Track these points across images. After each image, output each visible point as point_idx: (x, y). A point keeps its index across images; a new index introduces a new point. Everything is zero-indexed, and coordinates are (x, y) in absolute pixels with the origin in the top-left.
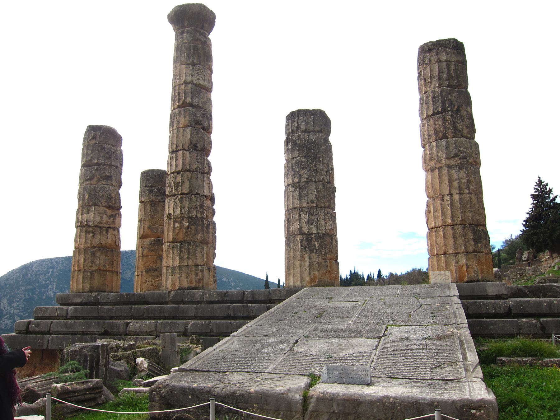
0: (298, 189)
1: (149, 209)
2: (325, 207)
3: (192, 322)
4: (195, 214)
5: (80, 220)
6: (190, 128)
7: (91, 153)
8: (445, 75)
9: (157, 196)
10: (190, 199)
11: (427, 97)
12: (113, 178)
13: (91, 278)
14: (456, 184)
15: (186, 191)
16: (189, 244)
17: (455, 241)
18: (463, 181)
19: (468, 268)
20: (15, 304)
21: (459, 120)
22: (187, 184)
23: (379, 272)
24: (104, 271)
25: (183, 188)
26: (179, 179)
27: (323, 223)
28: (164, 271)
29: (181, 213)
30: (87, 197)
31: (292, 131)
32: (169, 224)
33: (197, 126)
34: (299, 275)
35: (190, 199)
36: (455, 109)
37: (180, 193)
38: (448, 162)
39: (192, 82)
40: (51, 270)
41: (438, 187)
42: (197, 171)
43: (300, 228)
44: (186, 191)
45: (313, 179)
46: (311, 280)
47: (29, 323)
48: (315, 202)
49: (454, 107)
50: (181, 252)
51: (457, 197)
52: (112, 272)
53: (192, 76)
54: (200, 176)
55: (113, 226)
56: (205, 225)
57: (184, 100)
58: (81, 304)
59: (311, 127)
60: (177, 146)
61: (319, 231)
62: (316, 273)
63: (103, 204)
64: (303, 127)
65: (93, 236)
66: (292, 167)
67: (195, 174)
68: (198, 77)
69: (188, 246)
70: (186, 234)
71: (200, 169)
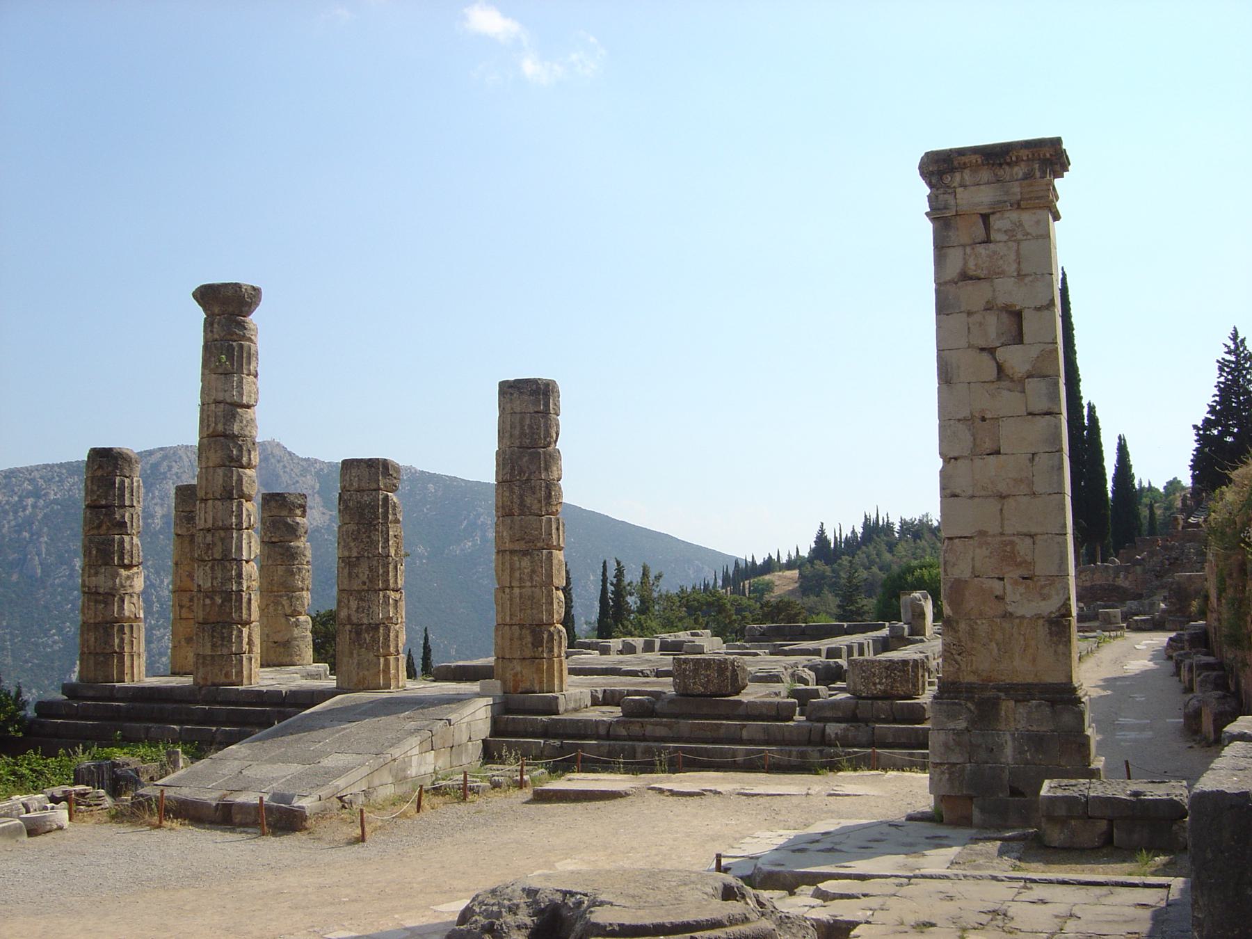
8: (517, 432)
40: (30, 501)
43: (349, 616)
44: (218, 556)
50: (213, 637)
51: (517, 591)
59: (364, 485)
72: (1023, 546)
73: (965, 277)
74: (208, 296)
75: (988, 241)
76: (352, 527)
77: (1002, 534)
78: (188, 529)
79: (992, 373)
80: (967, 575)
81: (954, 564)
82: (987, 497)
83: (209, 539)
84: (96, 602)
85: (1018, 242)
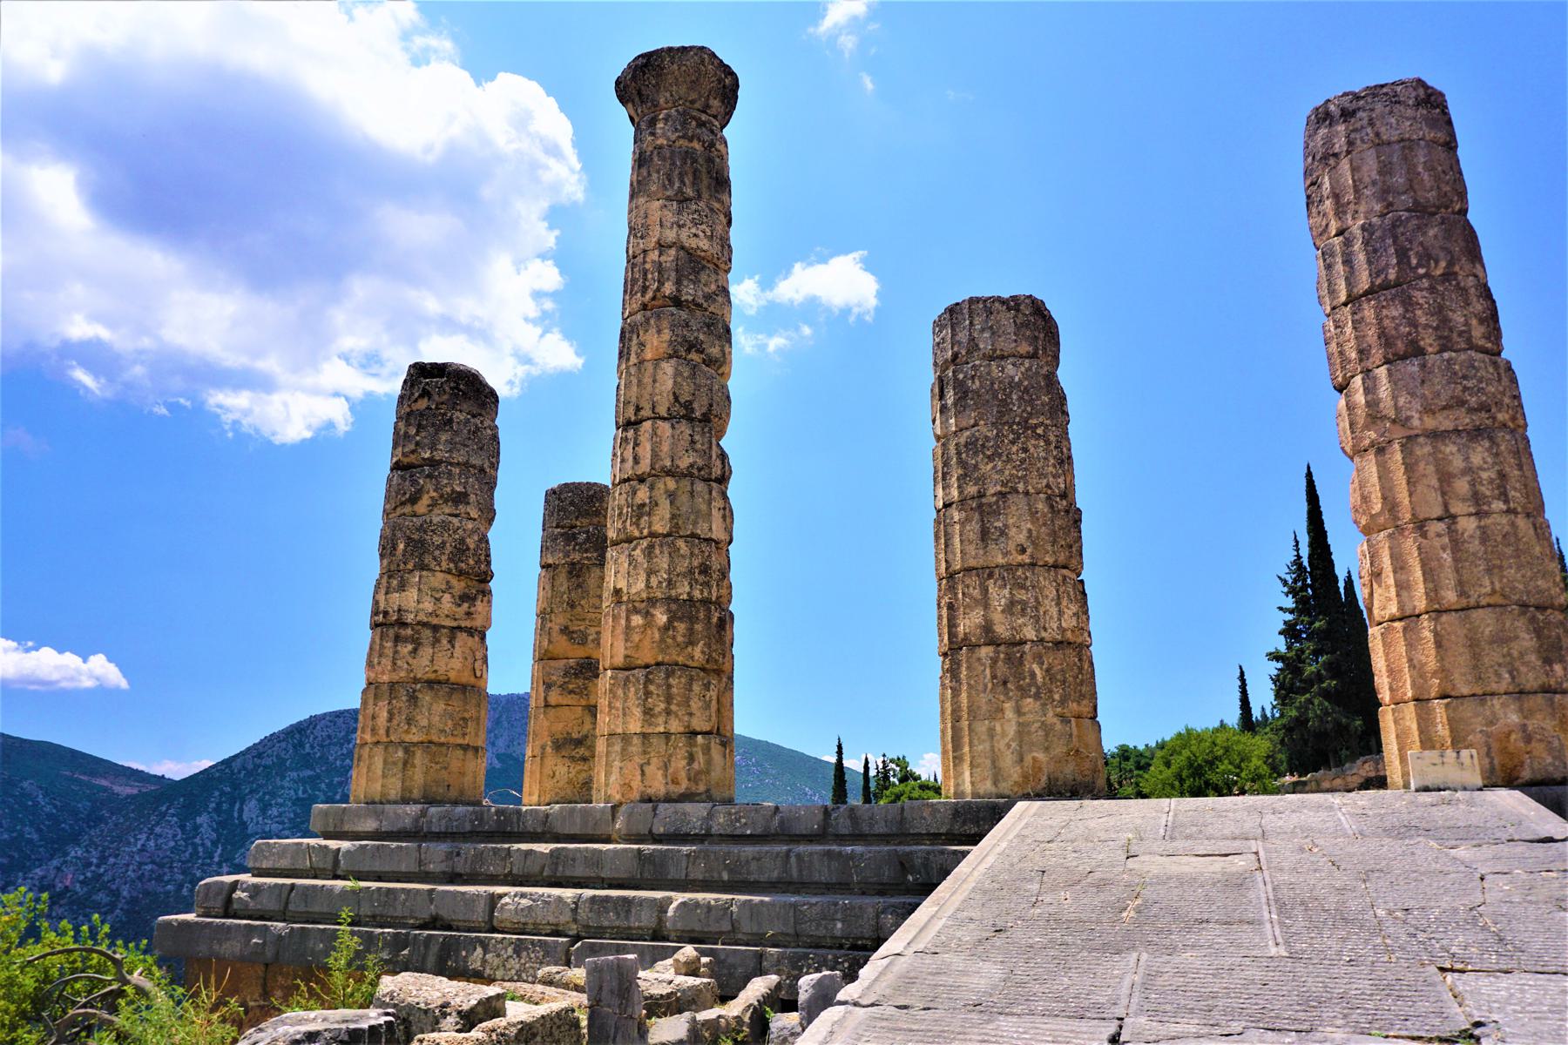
0: (977, 516)
1: (563, 583)
2: (1055, 566)
3: (680, 898)
4: (687, 589)
5: (382, 606)
6: (674, 361)
7: (417, 433)
8: (1399, 180)
9: (586, 551)
10: (673, 552)
11: (1348, 243)
12: (472, 498)
13: (405, 763)
14: (1462, 486)
16: (669, 675)
17: (1476, 657)
18: (1485, 475)
19: (1528, 739)
20: (274, 811)
21: (1452, 301)
22: (664, 510)
24: (442, 744)
25: (655, 519)
27: (1054, 611)
28: (601, 746)
29: (648, 586)
30: (401, 546)
31: (955, 356)
32: (615, 618)
33: (694, 356)
34: (988, 762)
36: (1439, 272)
37: (645, 532)
38: (1430, 423)
41: (1403, 496)
42: (691, 475)
43: (987, 628)
44: (660, 527)
45: (1021, 487)
46: (1025, 777)
48: (1029, 551)
49: (1437, 263)
50: (648, 694)
51: (1468, 525)
52: (465, 748)
53: (680, 227)
54: (700, 487)
55: (468, 624)
56: (715, 620)
57: (658, 289)
58: (376, 835)
60: (638, 409)
61: (1044, 634)
62: (1041, 756)
63: (444, 565)
64: (985, 345)
65: (415, 651)
66: (959, 453)
67: (686, 483)
68: (694, 230)
69: (668, 677)
70: (662, 645)
71: (700, 470)
74: (643, 82)
76: (985, 430)
78: (567, 555)
83: (643, 494)
84: (397, 639)
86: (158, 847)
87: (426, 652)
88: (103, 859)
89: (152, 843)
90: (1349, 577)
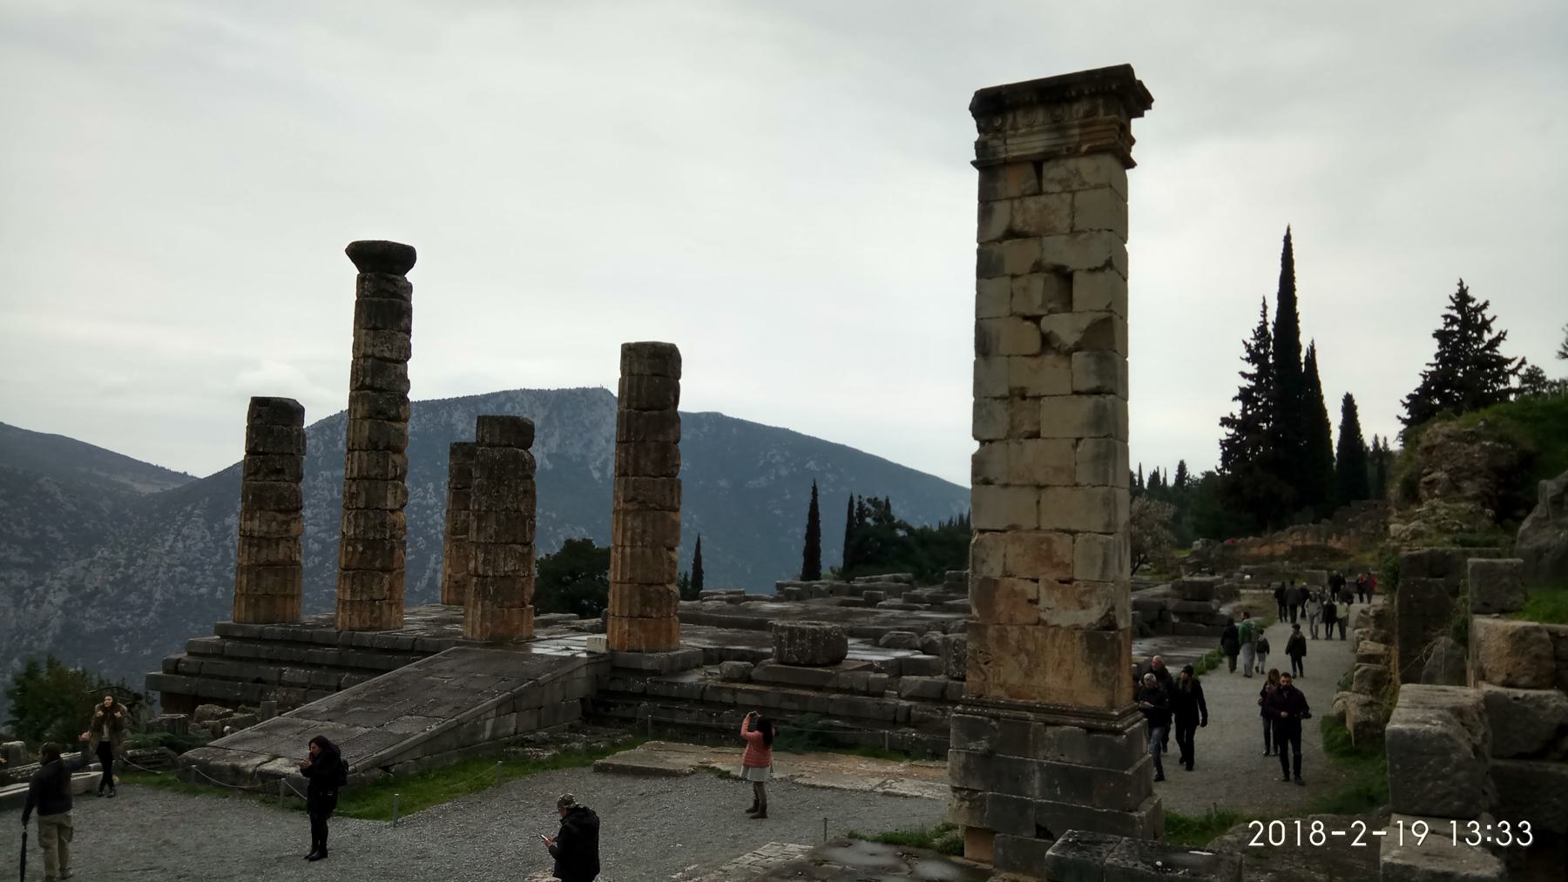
10: (367, 517)
14: (629, 534)
15: (362, 505)
22: (363, 496)
23: (1182, 467)
26: (354, 489)
35: (367, 517)
39: (373, 356)
44: (362, 505)
47: (179, 661)
51: (628, 550)
52: (285, 597)
54: (381, 484)
72: (1061, 545)
73: (1011, 234)
74: (358, 252)
75: (1039, 192)
77: (1038, 529)
79: (1034, 344)
80: (997, 574)
81: (984, 561)
82: (1022, 486)
85: (1073, 193)
86: (187, 549)
87: (264, 552)
88: (131, 561)
89: (180, 545)
90: (1312, 348)
